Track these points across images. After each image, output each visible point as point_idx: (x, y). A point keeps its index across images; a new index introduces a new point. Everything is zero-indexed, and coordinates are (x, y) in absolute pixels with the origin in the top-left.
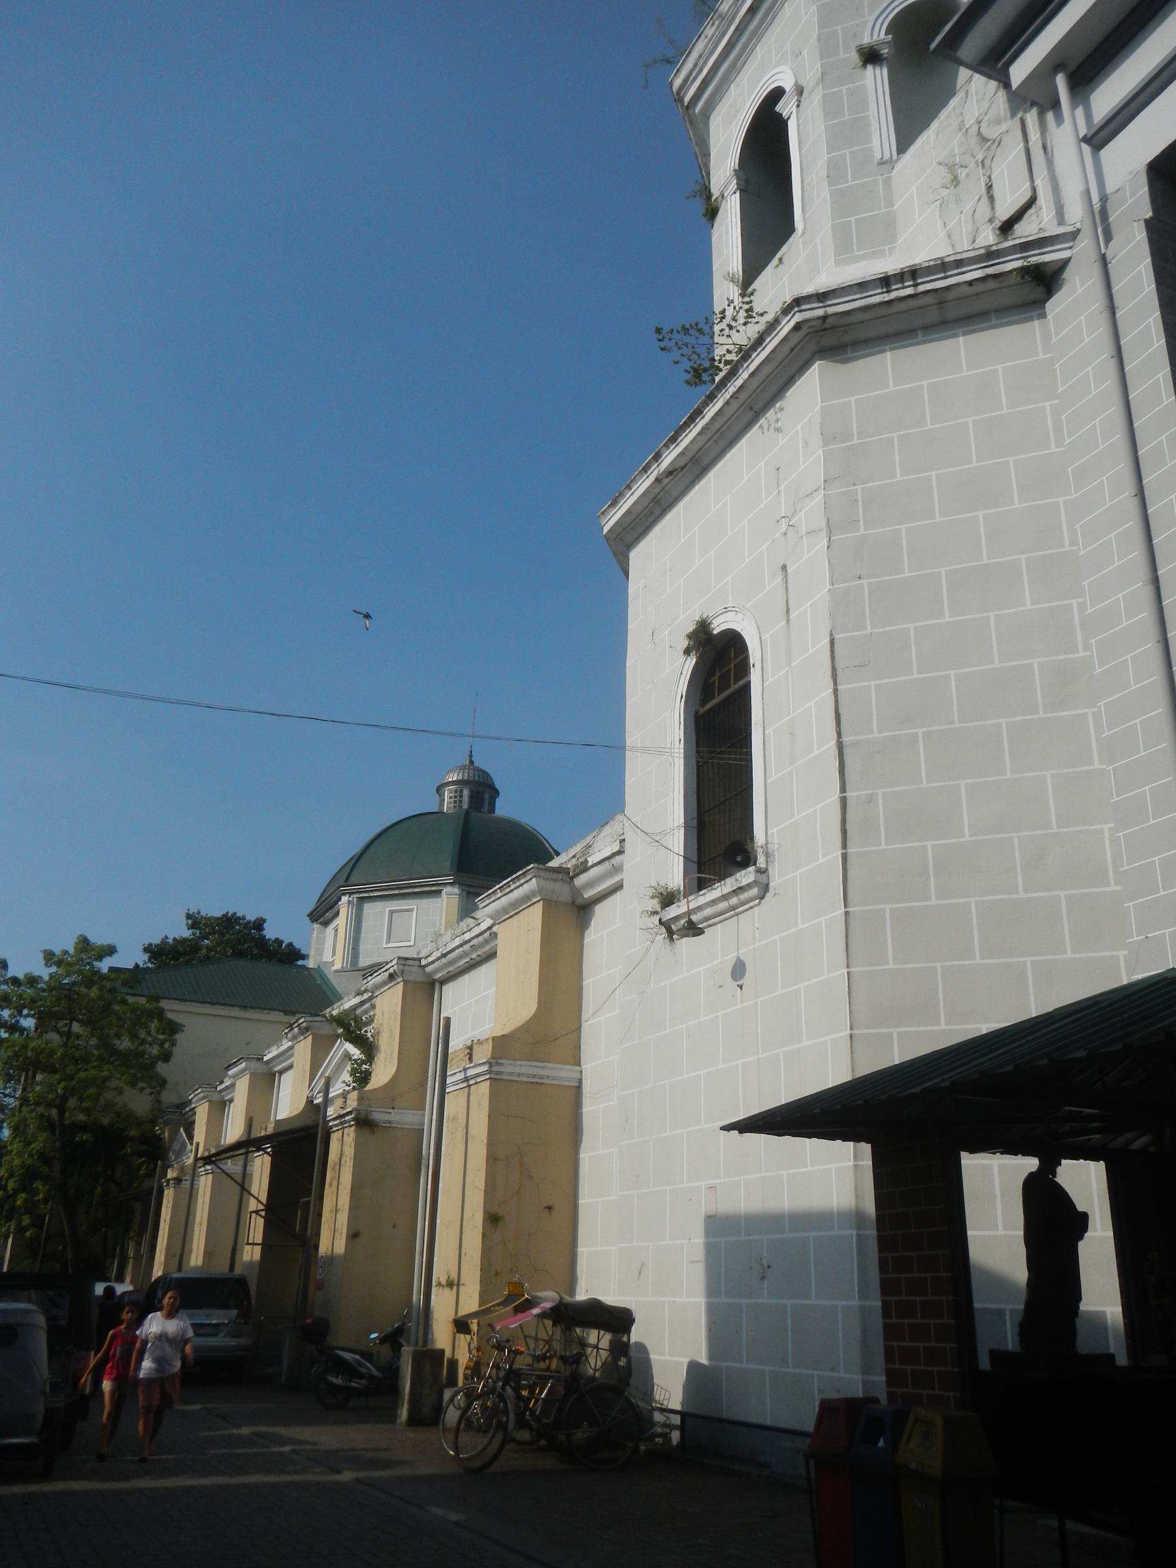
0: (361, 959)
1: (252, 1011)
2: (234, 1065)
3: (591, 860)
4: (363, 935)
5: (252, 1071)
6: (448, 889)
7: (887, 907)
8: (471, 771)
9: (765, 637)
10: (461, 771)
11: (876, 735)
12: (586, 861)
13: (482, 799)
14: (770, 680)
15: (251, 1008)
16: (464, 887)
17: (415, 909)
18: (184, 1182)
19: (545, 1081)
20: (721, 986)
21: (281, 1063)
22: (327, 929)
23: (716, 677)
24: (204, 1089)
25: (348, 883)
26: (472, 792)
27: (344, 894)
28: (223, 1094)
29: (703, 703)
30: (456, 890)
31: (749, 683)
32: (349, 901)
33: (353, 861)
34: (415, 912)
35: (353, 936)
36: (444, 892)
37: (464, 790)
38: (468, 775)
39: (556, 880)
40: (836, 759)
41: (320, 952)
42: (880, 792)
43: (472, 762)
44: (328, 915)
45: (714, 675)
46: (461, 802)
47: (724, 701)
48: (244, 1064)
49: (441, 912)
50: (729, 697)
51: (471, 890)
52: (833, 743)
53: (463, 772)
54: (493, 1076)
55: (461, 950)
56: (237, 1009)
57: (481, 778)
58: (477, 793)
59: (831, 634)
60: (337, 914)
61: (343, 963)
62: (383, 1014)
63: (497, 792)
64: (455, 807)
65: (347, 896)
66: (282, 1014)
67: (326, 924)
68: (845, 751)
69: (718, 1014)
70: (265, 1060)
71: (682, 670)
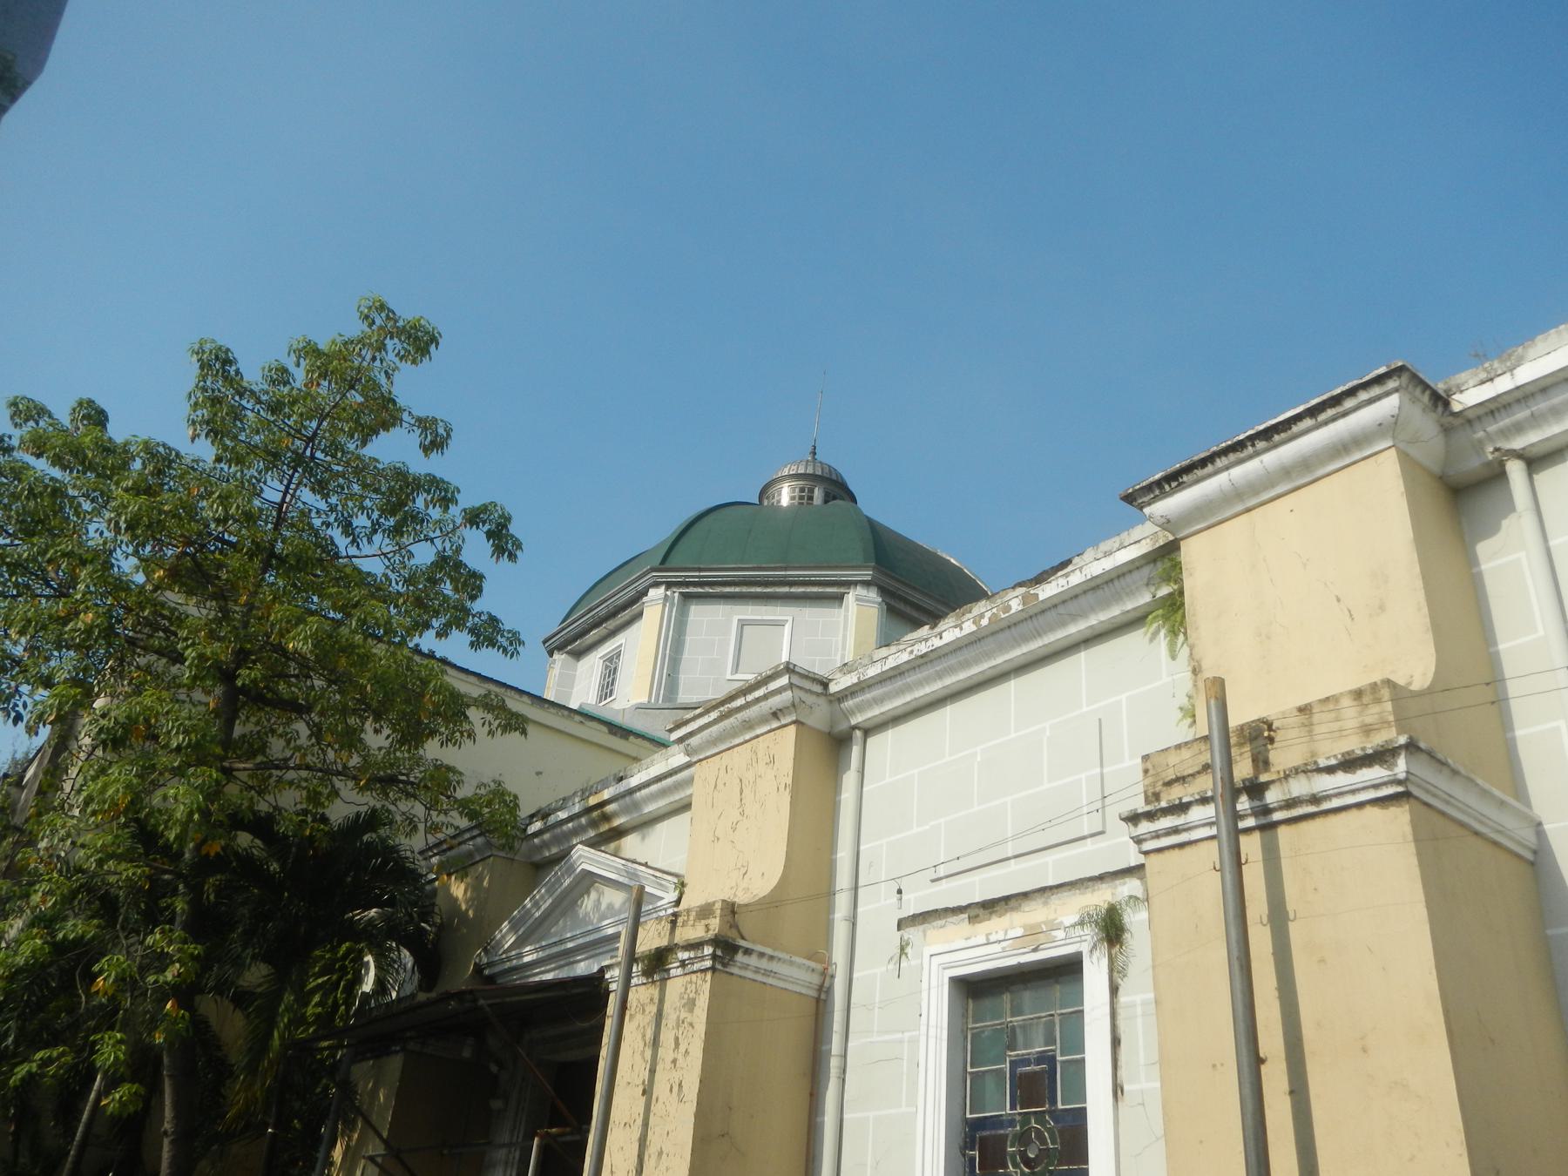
0: (680, 695)
1: (552, 710)
2: (1232, 457)
4: (686, 655)
6: (860, 591)
18: (740, 957)
21: (1536, 421)
22: (581, 662)
24: (795, 680)
25: (667, 565)
27: (656, 585)
28: (849, 704)
30: (873, 594)
34: (788, 627)
37: (816, 490)
38: (822, 469)
48: (1394, 400)
56: (525, 699)
60: (640, 615)
65: (663, 587)
66: (605, 729)
67: (578, 655)
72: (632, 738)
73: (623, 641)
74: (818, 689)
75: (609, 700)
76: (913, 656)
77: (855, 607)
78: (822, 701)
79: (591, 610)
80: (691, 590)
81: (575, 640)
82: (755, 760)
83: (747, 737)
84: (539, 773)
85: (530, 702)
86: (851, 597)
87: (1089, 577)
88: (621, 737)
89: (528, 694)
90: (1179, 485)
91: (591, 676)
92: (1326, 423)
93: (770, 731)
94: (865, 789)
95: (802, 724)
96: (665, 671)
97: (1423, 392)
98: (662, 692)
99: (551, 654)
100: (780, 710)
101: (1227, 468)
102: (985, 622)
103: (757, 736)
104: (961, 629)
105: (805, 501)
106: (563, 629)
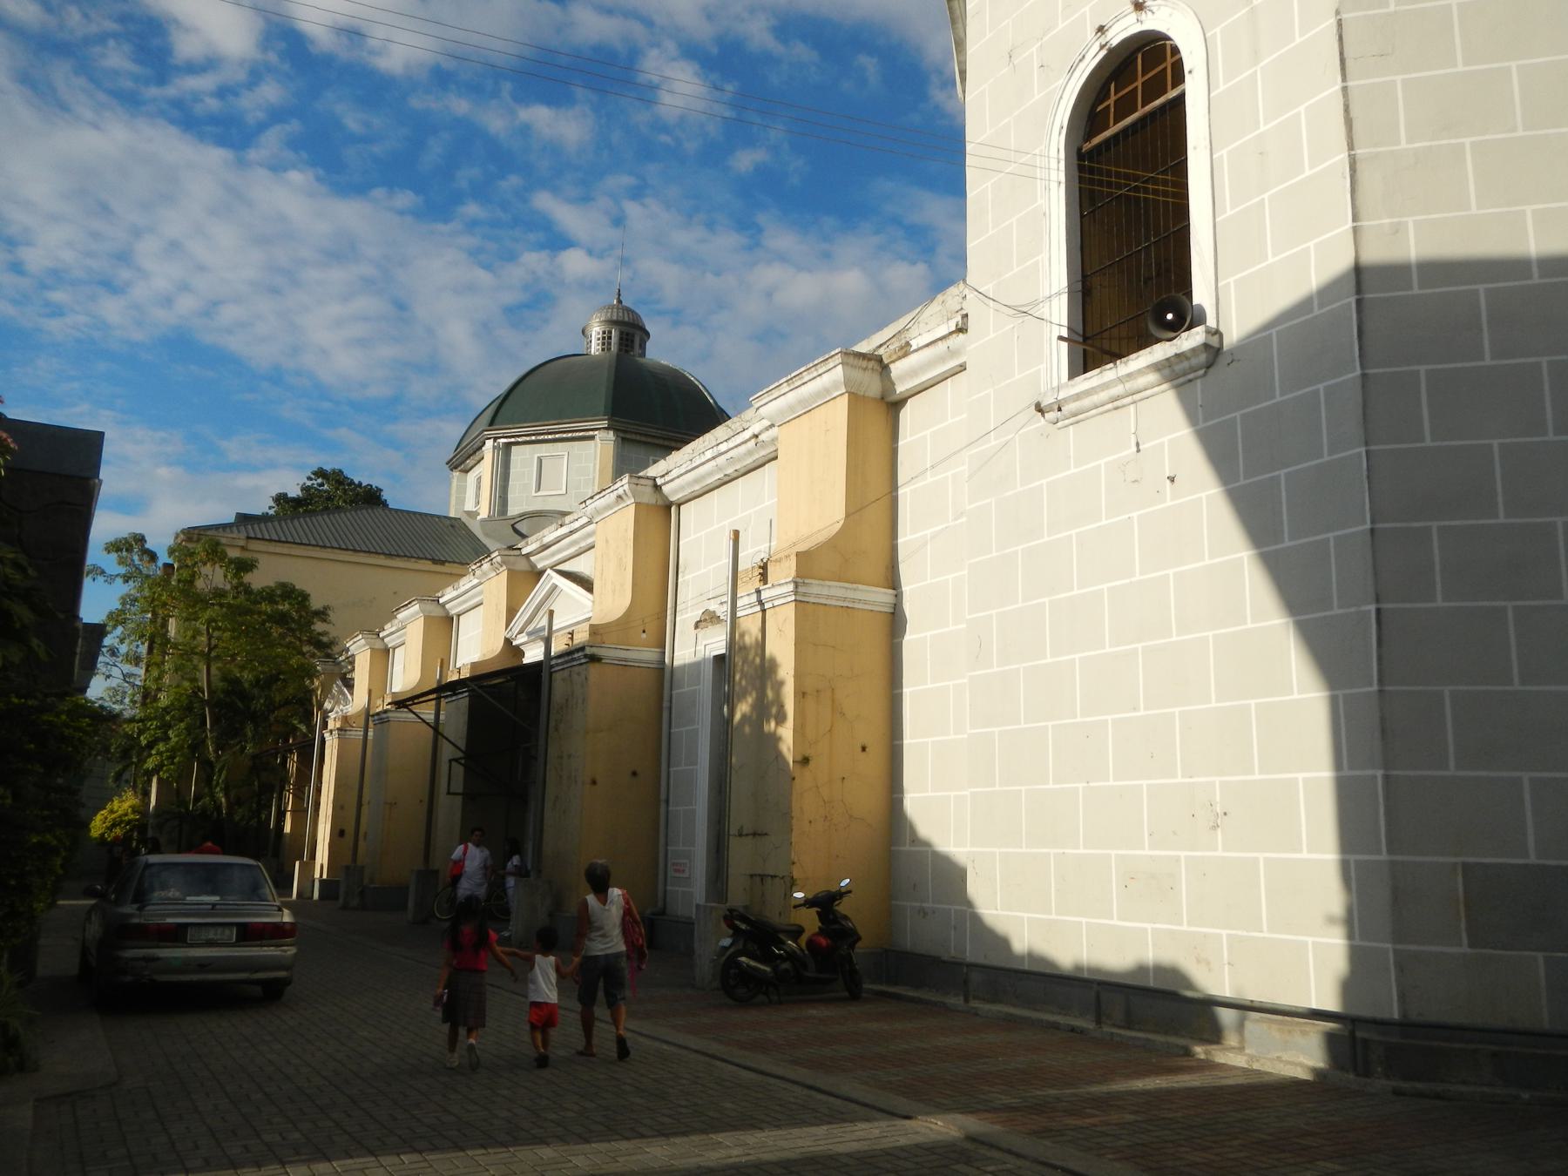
3: (915, 344)
5: (427, 614)
7: (1423, 368)
9: (1212, 32)
10: (610, 310)
11: (1404, 145)
12: (908, 344)
13: (632, 341)
14: (1221, 87)
17: (566, 457)
19: (856, 606)
20: (1136, 481)
23: (1111, 101)
26: (621, 333)
27: (490, 438)
29: (1088, 138)
31: (1181, 98)
32: (494, 447)
33: (499, 401)
36: (597, 438)
37: (613, 331)
39: (865, 369)
40: (1345, 178)
41: (462, 501)
42: (1410, 220)
43: (620, 302)
44: (470, 462)
45: (1107, 96)
46: (609, 344)
47: (1125, 130)
49: (595, 459)
50: (1134, 125)
51: (628, 436)
52: (1342, 157)
53: (612, 312)
54: (799, 598)
55: (713, 463)
58: (627, 334)
59: (1338, 12)
61: (490, 512)
62: (607, 541)
63: (648, 334)
64: (603, 350)
65: (492, 440)
66: (430, 562)
67: (467, 471)
68: (1359, 166)
69: (1130, 515)
70: (441, 601)
71: (1062, 94)
72: (447, 564)
78: (379, 641)
84: (395, 593)
105: (606, 341)
106: (456, 455)
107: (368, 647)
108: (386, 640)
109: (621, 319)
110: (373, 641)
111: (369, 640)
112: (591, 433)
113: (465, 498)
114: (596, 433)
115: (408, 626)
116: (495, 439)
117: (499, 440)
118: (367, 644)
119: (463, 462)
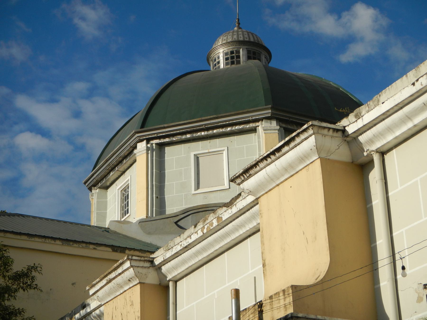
1: (75, 245)
2: (265, 162)
5: (323, 155)
8: (245, 33)
15: (75, 242)
16: (281, 123)
17: (225, 153)
24: (134, 263)
26: (249, 52)
27: (141, 141)
32: (148, 149)
35: (155, 184)
36: (260, 129)
41: (102, 216)
44: (113, 175)
48: (312, 139)
56: (58, 242)
57: (256, 39)
58: (254, 53)
66: (110, 249)
67: (107, 188)
73: (129, 178)
74: (148, 264)
75: (127, 215)
76: (182, 248)
77: (264, 134)
78: (151, 271)
79: (107, 161)
80: (162, 141)
81: (102, 179)
82: (126, 304)
83: (122, 292)
84: (73, 284)
85: (61, 243)
86: (261, 126)
87: (239, 210)
88: (121, 252)
89: (59, 239)
90: (250, 175)
91: (115, 202)
92: (293, 148)
93: (130, 288)
94: (178, 312)
95: (143, 283)
96: (154, 195)
97: (329, 131)
98: (154, 209)
99: (90, 189)
100: (131, 278)
101: (265, 167)
102: (205, 231)
103: (125, 291)
104: (197, 234)
105: (235, 60)
107: (138, 281)
108: (164, 269)
109: (248, 40)
110: (144, 271)
111: (140, 270)
112: (252, 125)
113: (106, 213)
114: (257, 124)
115: (261, 200)
116: (148, 141)
117: (152, 142)
118: (137, 275)
119: (105, 176)
